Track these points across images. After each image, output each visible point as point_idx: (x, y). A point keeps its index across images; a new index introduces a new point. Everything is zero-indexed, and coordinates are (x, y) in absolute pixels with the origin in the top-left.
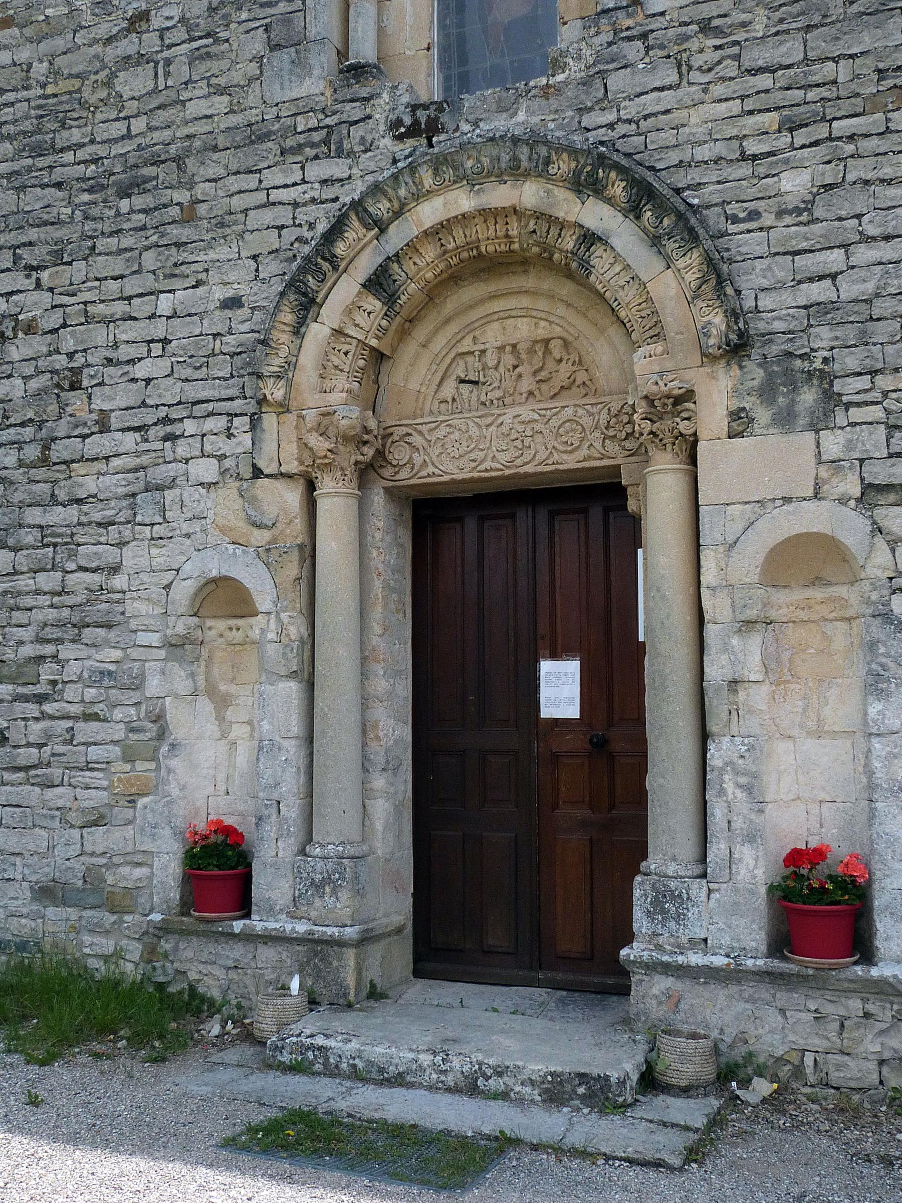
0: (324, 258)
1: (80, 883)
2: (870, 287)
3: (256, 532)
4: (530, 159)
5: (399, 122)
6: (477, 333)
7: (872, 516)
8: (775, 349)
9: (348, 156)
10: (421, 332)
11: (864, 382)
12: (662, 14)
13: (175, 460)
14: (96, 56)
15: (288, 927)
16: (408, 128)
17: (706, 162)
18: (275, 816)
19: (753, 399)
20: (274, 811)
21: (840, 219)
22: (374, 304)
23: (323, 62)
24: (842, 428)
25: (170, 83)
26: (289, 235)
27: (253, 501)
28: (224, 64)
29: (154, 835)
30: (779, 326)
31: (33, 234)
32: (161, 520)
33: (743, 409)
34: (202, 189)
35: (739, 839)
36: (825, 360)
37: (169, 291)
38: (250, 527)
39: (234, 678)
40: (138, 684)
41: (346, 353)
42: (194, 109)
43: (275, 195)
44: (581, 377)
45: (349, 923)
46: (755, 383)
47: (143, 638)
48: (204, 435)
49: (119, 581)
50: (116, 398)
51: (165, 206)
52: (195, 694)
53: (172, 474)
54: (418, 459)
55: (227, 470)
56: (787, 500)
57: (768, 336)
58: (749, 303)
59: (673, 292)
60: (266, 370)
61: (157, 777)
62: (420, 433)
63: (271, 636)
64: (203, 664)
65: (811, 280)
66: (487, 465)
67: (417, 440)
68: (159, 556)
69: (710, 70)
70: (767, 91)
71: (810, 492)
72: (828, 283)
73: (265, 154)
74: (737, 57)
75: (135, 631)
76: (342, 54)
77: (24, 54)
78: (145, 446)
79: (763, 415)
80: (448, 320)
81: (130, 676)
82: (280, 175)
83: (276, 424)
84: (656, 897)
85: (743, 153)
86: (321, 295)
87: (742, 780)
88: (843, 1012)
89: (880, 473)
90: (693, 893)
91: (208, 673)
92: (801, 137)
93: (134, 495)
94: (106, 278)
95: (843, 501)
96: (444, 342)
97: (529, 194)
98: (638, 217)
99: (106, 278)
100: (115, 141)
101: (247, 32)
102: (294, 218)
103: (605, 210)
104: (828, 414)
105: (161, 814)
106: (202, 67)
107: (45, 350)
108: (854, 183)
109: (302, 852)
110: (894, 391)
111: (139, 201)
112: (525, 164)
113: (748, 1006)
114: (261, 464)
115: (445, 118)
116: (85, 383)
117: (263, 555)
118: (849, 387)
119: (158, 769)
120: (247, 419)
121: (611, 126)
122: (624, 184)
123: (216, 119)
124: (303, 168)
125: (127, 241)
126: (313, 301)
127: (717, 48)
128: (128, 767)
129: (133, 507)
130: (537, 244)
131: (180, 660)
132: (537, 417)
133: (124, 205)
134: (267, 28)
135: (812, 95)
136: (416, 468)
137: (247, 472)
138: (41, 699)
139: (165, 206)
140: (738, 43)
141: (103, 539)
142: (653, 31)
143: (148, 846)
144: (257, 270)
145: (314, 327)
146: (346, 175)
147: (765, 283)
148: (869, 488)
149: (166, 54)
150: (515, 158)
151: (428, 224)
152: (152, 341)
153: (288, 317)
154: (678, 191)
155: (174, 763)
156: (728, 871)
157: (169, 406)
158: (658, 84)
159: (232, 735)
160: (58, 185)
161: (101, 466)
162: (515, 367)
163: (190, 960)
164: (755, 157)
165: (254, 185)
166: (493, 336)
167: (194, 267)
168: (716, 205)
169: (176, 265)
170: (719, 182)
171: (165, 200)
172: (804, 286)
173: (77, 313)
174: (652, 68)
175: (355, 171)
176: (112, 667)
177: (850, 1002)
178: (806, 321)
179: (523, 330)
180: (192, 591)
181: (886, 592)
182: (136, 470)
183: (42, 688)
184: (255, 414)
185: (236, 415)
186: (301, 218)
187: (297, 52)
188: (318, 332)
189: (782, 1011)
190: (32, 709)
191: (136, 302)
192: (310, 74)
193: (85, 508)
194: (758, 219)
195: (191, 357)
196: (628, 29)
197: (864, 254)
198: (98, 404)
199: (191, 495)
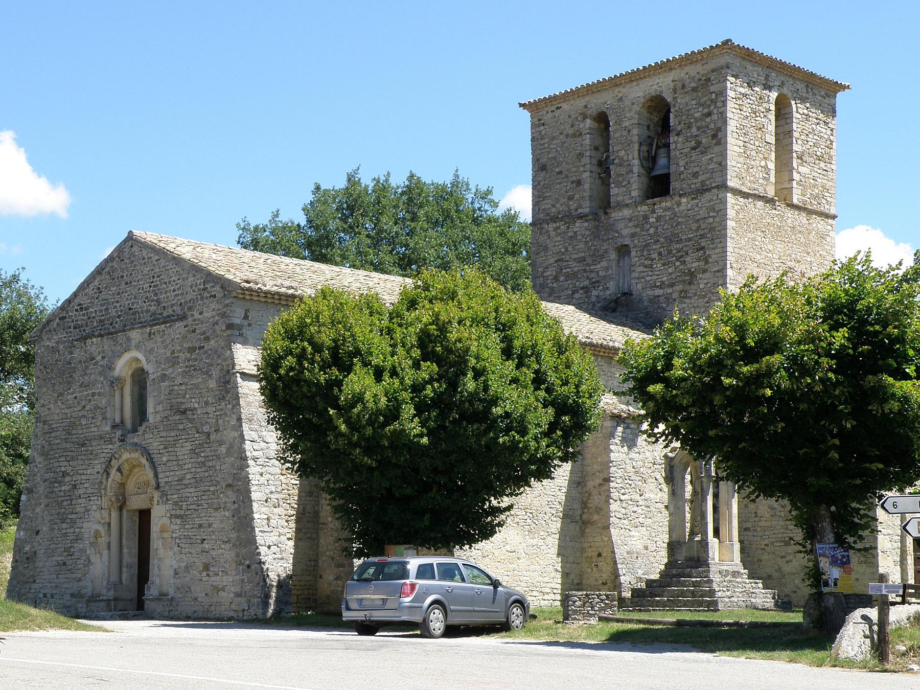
31: (69, 453)
42: (92, 430)
50: (81, 491)
77: (66, 411)
153: (105, 477)
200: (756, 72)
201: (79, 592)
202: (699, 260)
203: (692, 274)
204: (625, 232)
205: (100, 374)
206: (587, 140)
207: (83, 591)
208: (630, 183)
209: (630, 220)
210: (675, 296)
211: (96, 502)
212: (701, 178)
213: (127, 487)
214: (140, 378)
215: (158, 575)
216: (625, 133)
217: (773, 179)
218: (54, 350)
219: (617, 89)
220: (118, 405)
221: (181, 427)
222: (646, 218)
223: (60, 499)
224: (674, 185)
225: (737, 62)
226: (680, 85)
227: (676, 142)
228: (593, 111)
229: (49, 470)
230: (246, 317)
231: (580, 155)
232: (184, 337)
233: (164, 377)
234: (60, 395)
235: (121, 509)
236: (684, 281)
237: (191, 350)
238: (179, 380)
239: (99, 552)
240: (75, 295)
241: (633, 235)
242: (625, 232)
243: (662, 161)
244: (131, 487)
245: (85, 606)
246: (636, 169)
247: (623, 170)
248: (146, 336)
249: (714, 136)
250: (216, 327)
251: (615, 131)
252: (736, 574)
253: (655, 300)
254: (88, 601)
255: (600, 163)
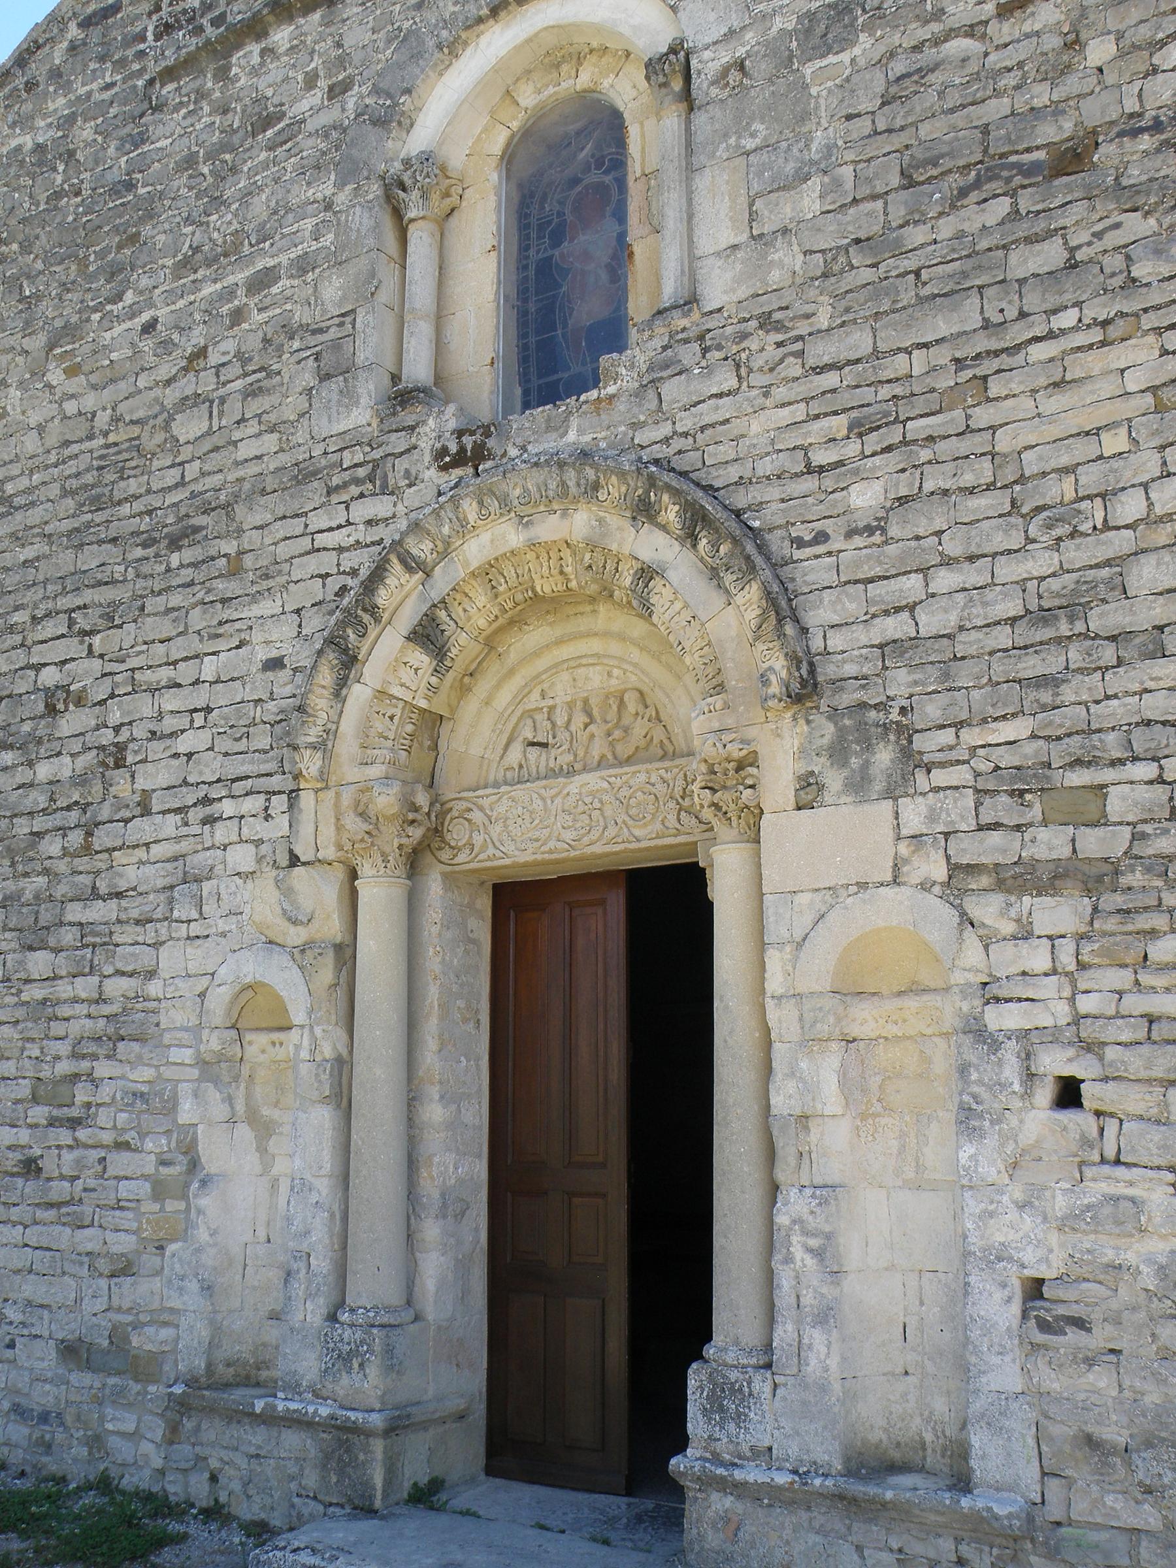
0: (365, 610)
1: (106, 1343)
2: (953, 619)
3: (292, 930)
4: (578, 485)
5: (444, 451)
6: (545, 686)
7: (961, 905)
8: (847, 699)
9: (392, 493)
10: (482, 688)
11: (946, 737)
12: (720, 310)
13: (213, 847)
14: (156, 400)
15: (311, 1409)
16: (454, 456)
17: (768, 478)
18: (304, 1271)
19: (823, 760)
20: (302, 1265)
21: (918, 538)
22: (420, 658)
23: (370, 389)
24: (924, 794)
25: (224, 423)
26: (334, 584)
27: (287, 892)
28: (275, 399)
29: (181, 1289)
30: (850, 669)
31: (88, 596)
32: (197, 916)
33: (812, 773)
34: (252, 539)
35: (809, 1319)
36: (903, 711)
37: (213, 654)
38: (287, 924)
39: (278, 1102)
40: (171, 1107)
41: (391, 718)
43: (322, 540)
44: (658, 734)
45: (378, 1406)
46: (825, 741)
47: (176, 1055)
48: (242, 817)
49: (154, 988)
50: (156, 775)
51: (213, 559)
52: (232, 1121)
53: (210, 862)
54: (478, 840)
55: (264, 857)
56: (862, 886)
57: (838, 683)
58: (817, 644)
59: (733, 633)
60: (301, 740)
61: (187, 1219)
62: (481, 809)
63: (304, 1054)
64: (243, 1085)
65: (886, 613)
66: (552, 844)
67: (477, 816)
68: (196, 957)
69: (771, 370)
70: (834, 391)
71: (889, 877)
72: (905, 615)
73: (310, 495)
74: (800, 354)
75: (169, 1046)
76: (395, 378)
77: (90, 402)
78: (185, 830)
79: (834, 780)
80: (511, 672)
81: (162, 1101)
82: (325, 517)
83: (313, 802)
84: (713, 1391)
85: (808, 465)
86: (364, 651)
87: (813, 1243)
88: (932, 1554)
89: (968, 850)
90: (756, 1386)
91: (249, 1096)
92: (873, 441)
93: (172, 887)
94: (153, 642)
95: (925, 886)
96: (509, 698)
97: (580, 522)
98: (694, 546)
99: (153, 642)
100: (169, 489)
101: (299, 362)
102: (338, 565)
103: (660, 538)
104: (907, 778)
105: (189, 1263)
106: (255, 406)
107: (93, 723)
108: (932, 493)
109: (332, 1318)
110: (983, 746)
111: (188, 555)
112: (573, 490)
113: (818, 1539)
114: (298, 851)
115: (491, 443)
116: (130, 759)
117: (297, 956)
118: (928, 744)
119: (188, 1209)
120: (284, 797)
121: (666, 440)
122: (677, 507)
123: (265, 458)
124: (347, 508)
125: (175, 600)
126: (354, 659)
127: (779, 345)
128: (157, 1207)
129: (171, 901)
130: (594, 581)
131: (216, 1081)
132: (605, 785)
133: (175, 559)
134: (317, 357)
135: (885, 392)
136: (476, 850)
137: (284, 861)
138: (74, 1123)
139: (213, 559)
140: (800, 338)
141: (140, 939)
142: (709, 331)
143: (175, 1303)
144: (300, 626)
145: (357, 688)
146: (389, 514)
147: (836, 619)
148: (955, 869)
149: (221, 392)
150: (563, 484)
151: (474, 564)
152: (196, 710)
153: (326, 677)
154: (738, 514)
155: (203, 1202)
156: (795, 1360)
157: (210, 784)
158: (714, 391)
159: (275, 1171)
160: (114, 540)
161: (141, 853)
162: (586, 726)
163: (212, 1445)
164: (821, 469)
165: (299, 530)
166: (562, 690)
167: (238, 625)
168: (779, 527)
169: (220, 624)
170: (783, 501)
171: (213, 552)
172: (877, 621)
173: (125, 683)
174: (709, 370)
175: (400, 506)
176: (144, 1089)
177: (940, 1541)
178: (880, 664)
179: (595, 680)
180: (227, 999)
181: (978, 1002)
182: (175, 859)
183: (75, 1112)
184: (292, 791)
185: (274, 793)
186: (346, 566)
187: (345, 380)
188: (358, 694)
189: (859, 1549)
190: (64, 1136)
191: (181, 666)
192: (357, 403)
193: (124, 903)
194: (826, 541)
195: (232, 727)
196: (684, 330)
197: (944, 580)
198: (141, 783)
199: (228, 886)
201: (118, 1337)
207: (142, 1342)
211: (255, 828)
213: (454, 740)
215: (825, 1317)
220: (421, 292)
221: (1051, 254)
223: (22, 827)
239: (252, 1117)
244: (478, 735)
245: (157, 1430)
254: (182, 1406)
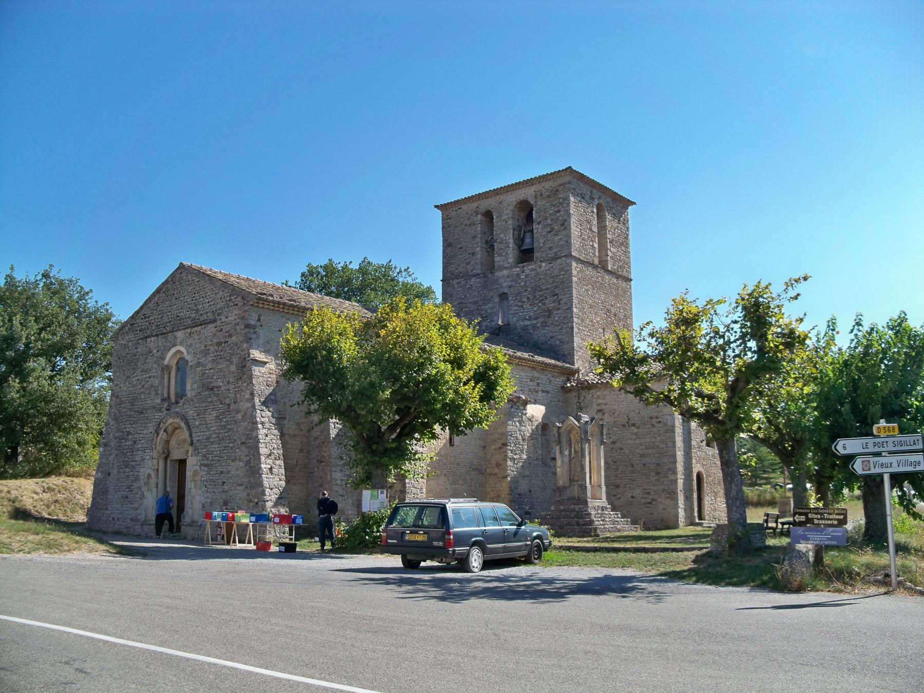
50: (139, 446)
200: (585, 189)
202: (554, 302)
203: (550, 312)
204: (505, 284)
205: (155, 362)
206: (479, 227)
208: (507, 253)
209: (508, 277)
210: (538, 325)
212: (554, 250)
214: (181, 364)
215: (191, 508)
216: (504, 223)
217: (597, 254)
218: (125, 346)
219: (498, 197)
220: (166, 384)
221: (210, 400)
222: (518, 275)
224: (536, 254)
225: (575, 181)
226: (539, 194)
227: (537, 229)
228: (482, 209)
229: (119, 430)
230: (259, 320)
231: (474, 237)
232: (214, 335)
233: (199, 364)
234: (128, 377)
235: (166, 458)
236: (544, 316)
237: (219, 344)
238: (209, 366)
240: (142, 308)
241: (510, 287)
242: (505, 284)
243: (528, 240)
244: (173, 443)
246: (511, 245)
247: (503, 246)
248: (187, 335)
249: (562, 225)
250: (238, 327)
251: (497, 222)
252: (603, 509)
253: (525, 328)
255: (487, 242)
